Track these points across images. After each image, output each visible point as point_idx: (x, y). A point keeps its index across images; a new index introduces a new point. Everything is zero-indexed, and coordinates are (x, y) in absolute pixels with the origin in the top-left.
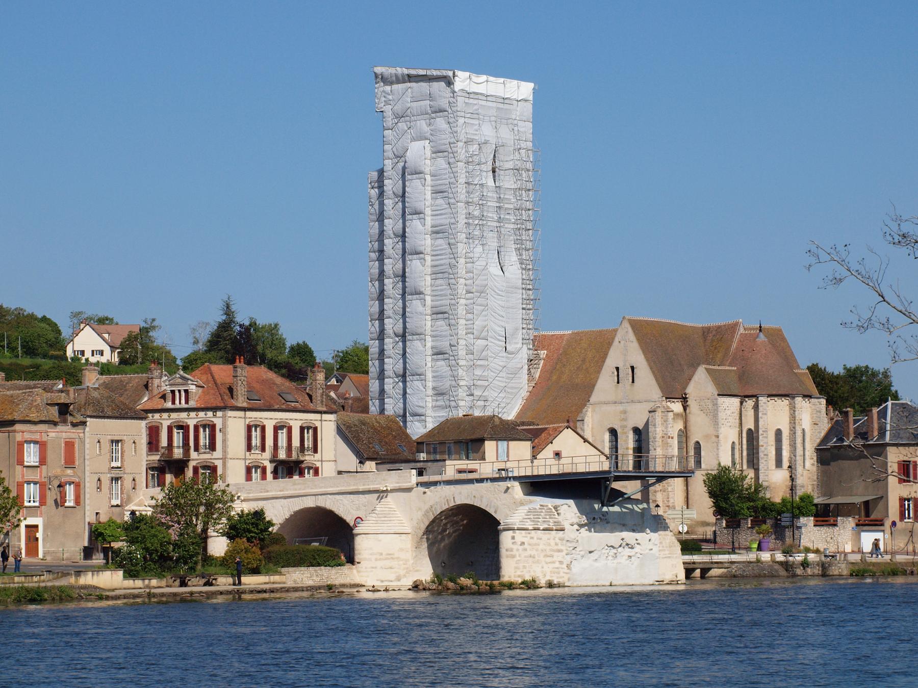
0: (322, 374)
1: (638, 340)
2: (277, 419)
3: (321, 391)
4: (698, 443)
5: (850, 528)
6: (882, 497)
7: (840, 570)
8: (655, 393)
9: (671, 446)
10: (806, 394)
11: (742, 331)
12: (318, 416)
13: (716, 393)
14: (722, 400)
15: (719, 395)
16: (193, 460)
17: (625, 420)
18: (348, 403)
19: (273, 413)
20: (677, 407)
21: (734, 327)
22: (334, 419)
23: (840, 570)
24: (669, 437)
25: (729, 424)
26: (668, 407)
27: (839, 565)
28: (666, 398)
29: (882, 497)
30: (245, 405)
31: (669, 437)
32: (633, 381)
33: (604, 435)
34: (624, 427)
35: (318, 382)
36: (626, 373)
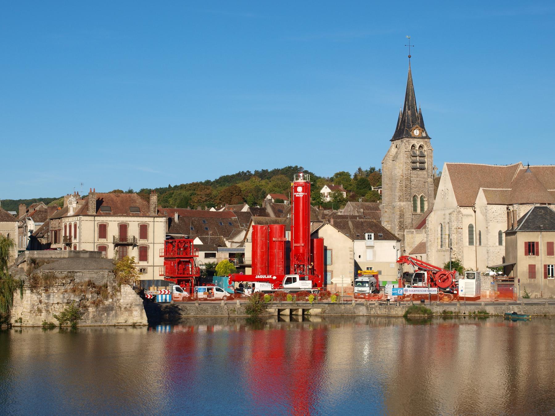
0: (155, 196)
1: (450, 175)
2: (139, 221)
3: (154, 206)
4: (480, 232)
5: (490, 283)
6: (515, 264)
7: (396, 312)
8: (455, 203)
9: (460, 233)
10: (542, 202)
11: (521, 167)
12: (152, 219)
13: (486, 203)
14: (490, 207)
15: (487, 204)
16: (73, 243)
17: (444, 219)
18: (321, 212)
19: (87, 217)
20: (469, 211)
21: (517, 166)
22: (164, 221)
23: (396, 312)
24: (459, 228)
25: (497, 221)
26: (460, 212)
27: (396, 309)
28: (460, 206)
29: (515, 264)
30: (95, 214)
31: (459, 228)
33: (438, 227)
34: (444, 222)
35: (152, 201)
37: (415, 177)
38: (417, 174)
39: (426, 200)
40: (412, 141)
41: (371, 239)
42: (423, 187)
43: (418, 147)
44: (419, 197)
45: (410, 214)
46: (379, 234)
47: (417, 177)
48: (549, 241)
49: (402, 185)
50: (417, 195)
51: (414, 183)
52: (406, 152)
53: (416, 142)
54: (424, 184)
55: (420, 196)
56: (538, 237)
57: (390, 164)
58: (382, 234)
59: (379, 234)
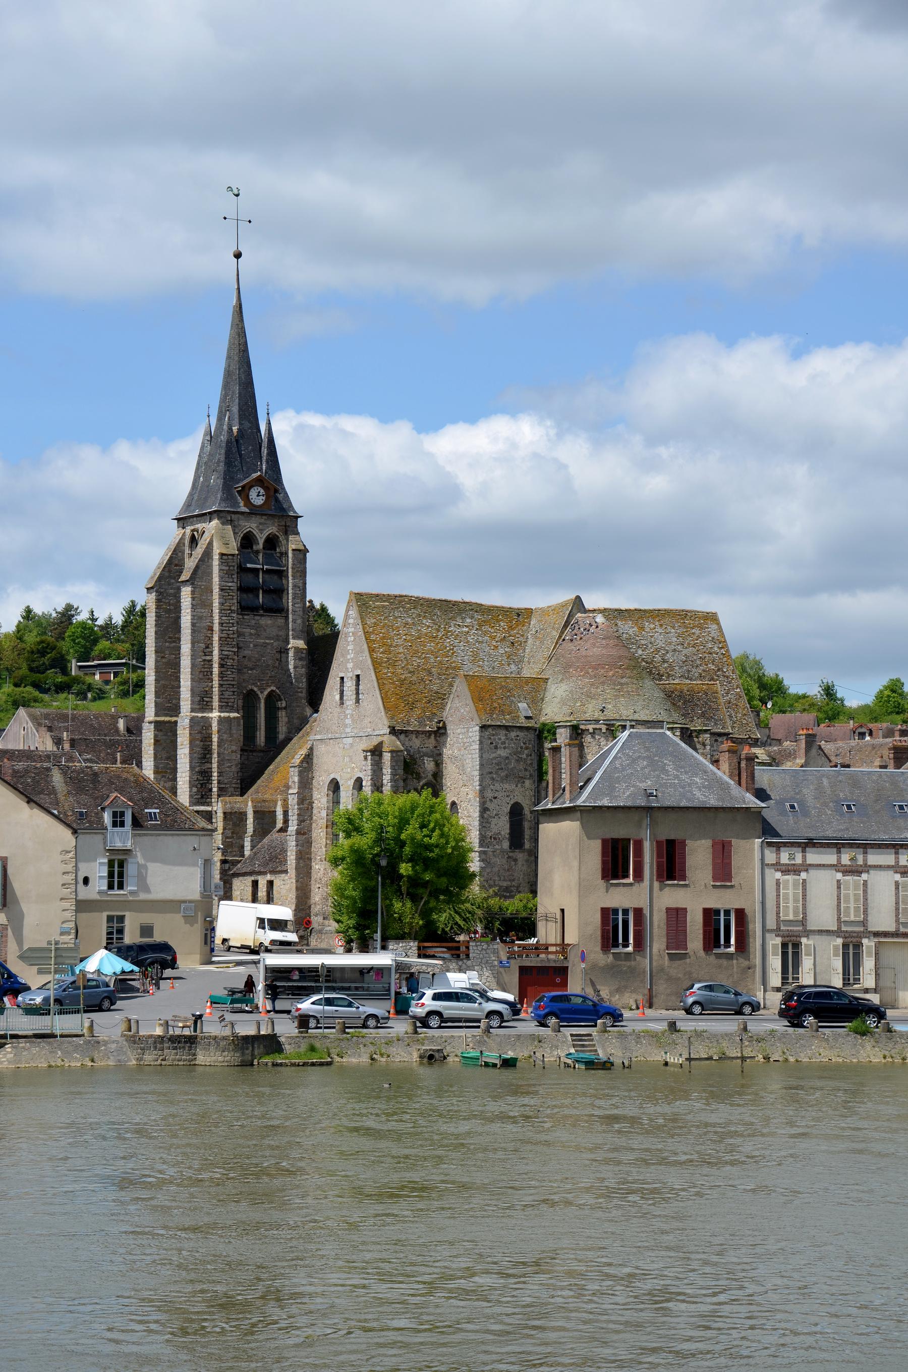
32: (358, 700)
36: (349, 685)
37: (251, 634)
38: (257, 627)
39: (284, 705)
40: (242, 523)
41: (122, 824)
42: (274, 667)
43: (261, 542)
44: (262, 696)
45: (234, 748)
46: (146, 811)
47: (258, 635)
48: (672, 837)
49: (208, 658)
50: (255, 689)
51: (247, 652)
52: (224, 557)
53: (254, 525)
54: (278, 655)
55: (266, 693)
56: (639, 825)
57: (172, 591)
58: (158, 811)
59: (146, 811)
